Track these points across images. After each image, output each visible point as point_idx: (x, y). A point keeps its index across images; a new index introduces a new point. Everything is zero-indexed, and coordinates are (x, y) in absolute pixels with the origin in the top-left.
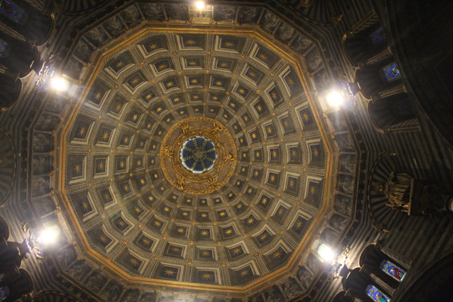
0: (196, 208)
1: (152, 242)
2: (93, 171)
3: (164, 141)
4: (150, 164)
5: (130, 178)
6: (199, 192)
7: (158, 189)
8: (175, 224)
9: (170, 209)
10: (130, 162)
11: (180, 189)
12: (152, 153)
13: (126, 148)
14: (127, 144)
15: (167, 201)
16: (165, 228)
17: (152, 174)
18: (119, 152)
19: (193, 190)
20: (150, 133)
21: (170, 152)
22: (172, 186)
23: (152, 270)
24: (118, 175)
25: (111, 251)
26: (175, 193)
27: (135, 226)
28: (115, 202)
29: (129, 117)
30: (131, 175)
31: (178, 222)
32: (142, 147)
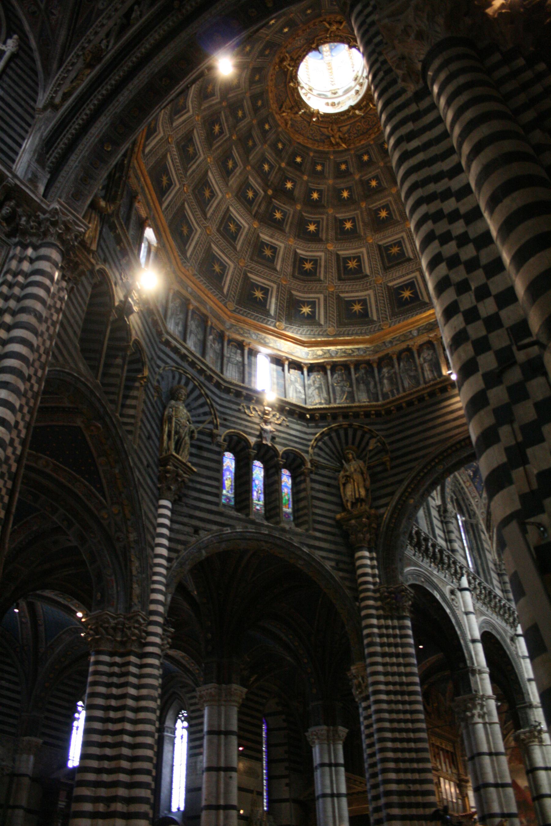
0: (382, 164)
1: (358, 259)
2: (231, 244)
3: (274, 106)
4: (278, 152)
5: (271, 197)
6: (370, 135)
7: (314, 173)
8: (370, 209)
9: (349, 189)
10: (256, 181)
11: (341, 149)
12: (272, 137)
13: (238, 171)
14: (235, 165)
15: (339, 181)
16: (361, 224)
17: (292, 163)
18: (234, 186)
19: (361, 137)
20: (247, 120)
21: (291, 108)
22: (327, 153)
23: (384, 304)
24: (257, 212)
25: (326, 317)
26: (339, 160)
27: (326, 254)
28: (280, 247)
29: (210, 138)
30: (270, 192)
31: (372, 204)
32: (255, 145)
